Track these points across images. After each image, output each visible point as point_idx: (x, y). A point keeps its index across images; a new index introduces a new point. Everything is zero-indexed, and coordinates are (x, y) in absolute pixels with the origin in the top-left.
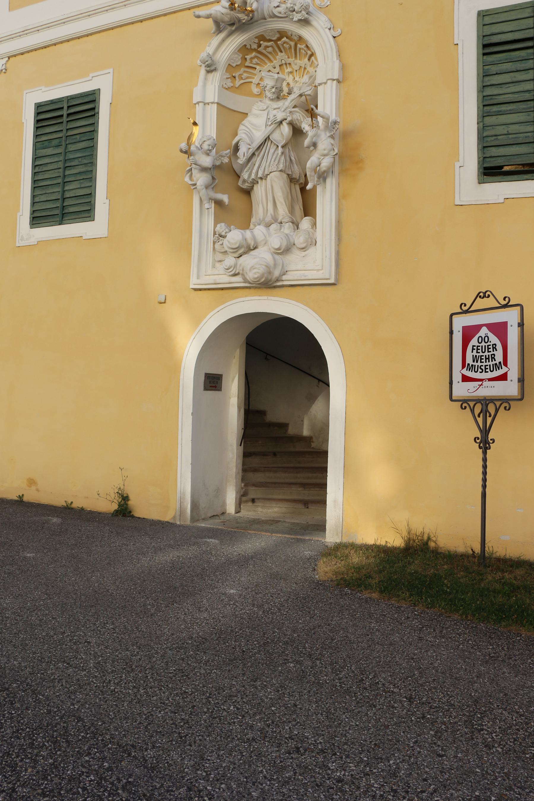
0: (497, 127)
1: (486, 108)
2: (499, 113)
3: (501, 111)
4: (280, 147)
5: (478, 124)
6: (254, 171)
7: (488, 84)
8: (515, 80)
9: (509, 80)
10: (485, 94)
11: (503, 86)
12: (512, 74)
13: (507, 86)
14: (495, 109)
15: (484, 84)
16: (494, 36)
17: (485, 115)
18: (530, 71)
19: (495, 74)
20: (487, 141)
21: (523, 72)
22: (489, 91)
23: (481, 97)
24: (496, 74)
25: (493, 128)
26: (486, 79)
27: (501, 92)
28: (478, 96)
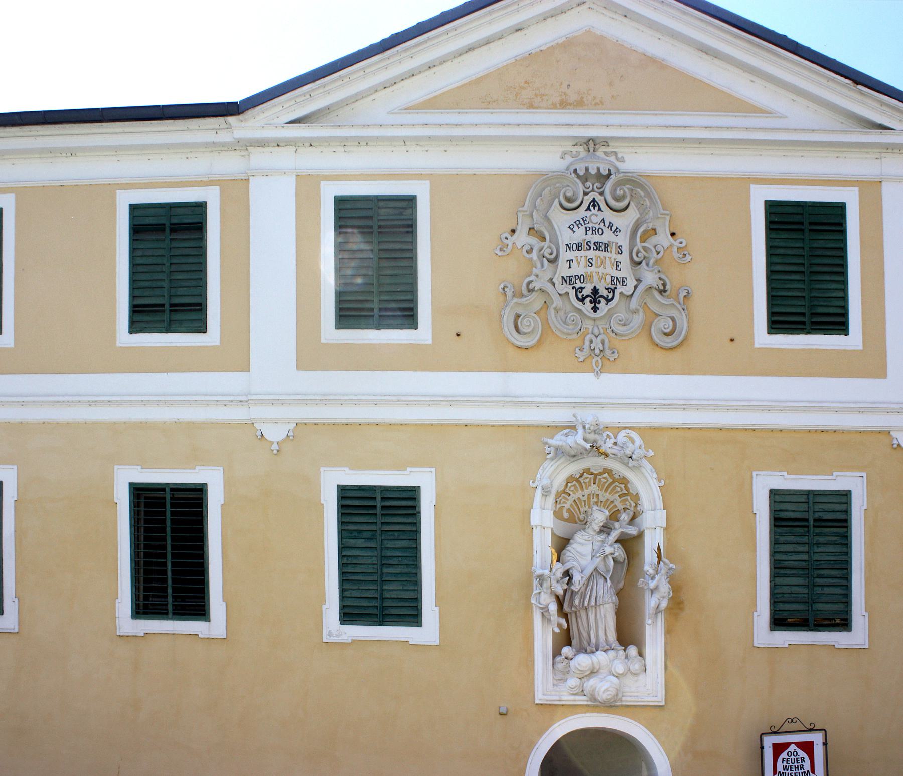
0: (784, 587)
1: (776, 570)
2: (786, 576)
3: (786, 574)
4: (608, 580)
5: (770, 582)
6: (587, 599)
7: (778, 550)
8: (796, 550)
9: (792, 550)
10: (775, 559)
11: (787, 554)
12: (794, 546)
13: (790, 554)
14: (782, 572)
15: (775, 551)
16: (782, 513)
17: (776, 576)
18: (806, 545)
19: (781, 544)
20: (777, 597)
21: (801, 546)
22: (778, 557)
23: (773, 561)
24: (784, 543)
25: (781, 588)
26: (777, 546)
27: (786, 559)
28: (770, 560)
